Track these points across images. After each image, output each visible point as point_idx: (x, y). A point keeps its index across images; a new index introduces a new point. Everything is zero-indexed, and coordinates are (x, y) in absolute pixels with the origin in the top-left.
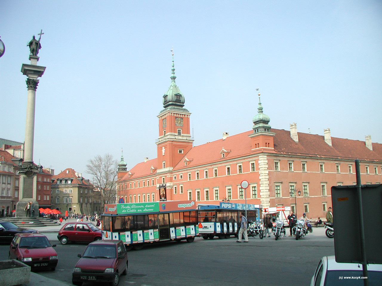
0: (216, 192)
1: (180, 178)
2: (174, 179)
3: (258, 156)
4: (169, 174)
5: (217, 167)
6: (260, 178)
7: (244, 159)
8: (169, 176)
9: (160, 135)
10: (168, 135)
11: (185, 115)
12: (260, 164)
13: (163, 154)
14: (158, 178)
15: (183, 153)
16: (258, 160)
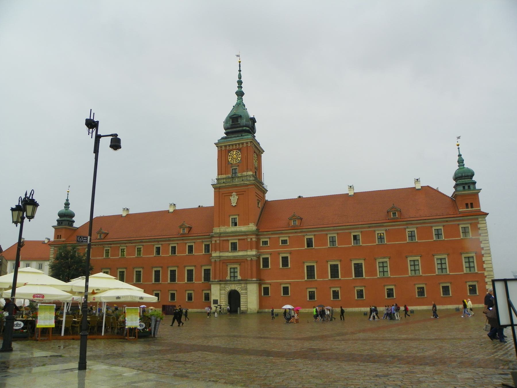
0: (381, 265)
1: (281, 244)
2: (261, 245)
3: (477, 219)
4: (254, 237)
5: (386, 230)
6: (482, 245)
7: (447, 221)
8: (254, 240)
9: (220, 172)
10: (250, 176)
11: (260, 151)
12: (481, 229)
13: (234, 204)
14: (218, 242)
15: (259, 206)
16: (478, 223)
